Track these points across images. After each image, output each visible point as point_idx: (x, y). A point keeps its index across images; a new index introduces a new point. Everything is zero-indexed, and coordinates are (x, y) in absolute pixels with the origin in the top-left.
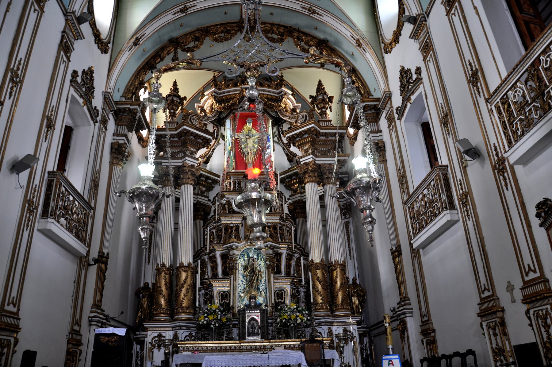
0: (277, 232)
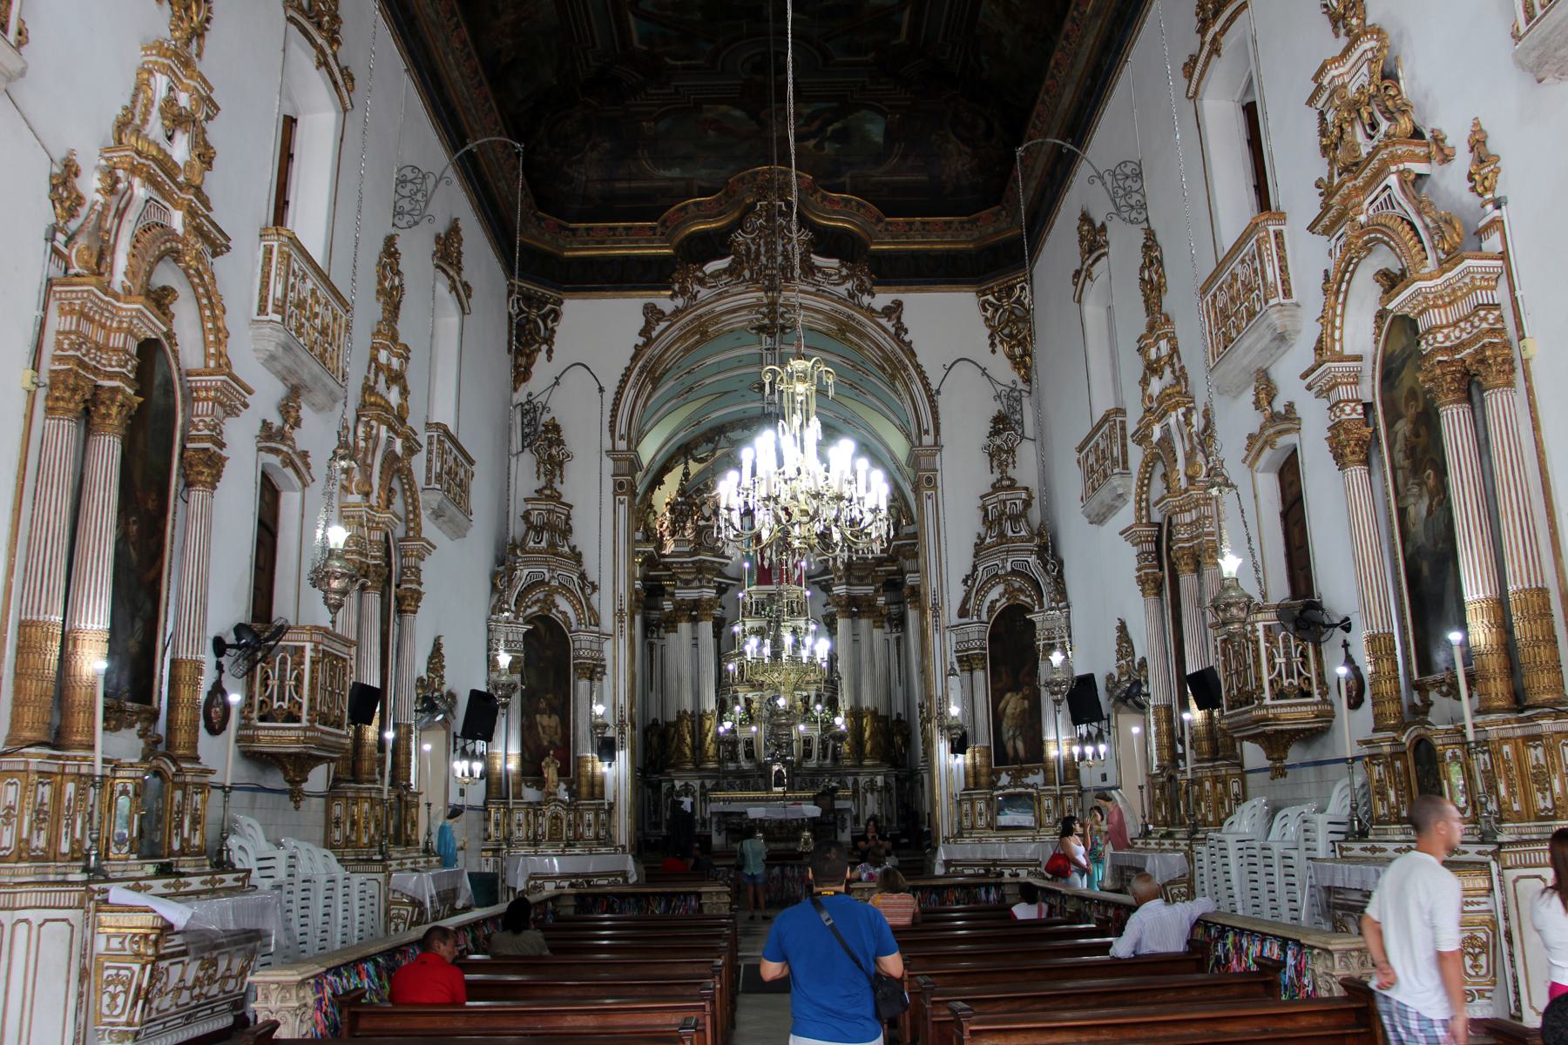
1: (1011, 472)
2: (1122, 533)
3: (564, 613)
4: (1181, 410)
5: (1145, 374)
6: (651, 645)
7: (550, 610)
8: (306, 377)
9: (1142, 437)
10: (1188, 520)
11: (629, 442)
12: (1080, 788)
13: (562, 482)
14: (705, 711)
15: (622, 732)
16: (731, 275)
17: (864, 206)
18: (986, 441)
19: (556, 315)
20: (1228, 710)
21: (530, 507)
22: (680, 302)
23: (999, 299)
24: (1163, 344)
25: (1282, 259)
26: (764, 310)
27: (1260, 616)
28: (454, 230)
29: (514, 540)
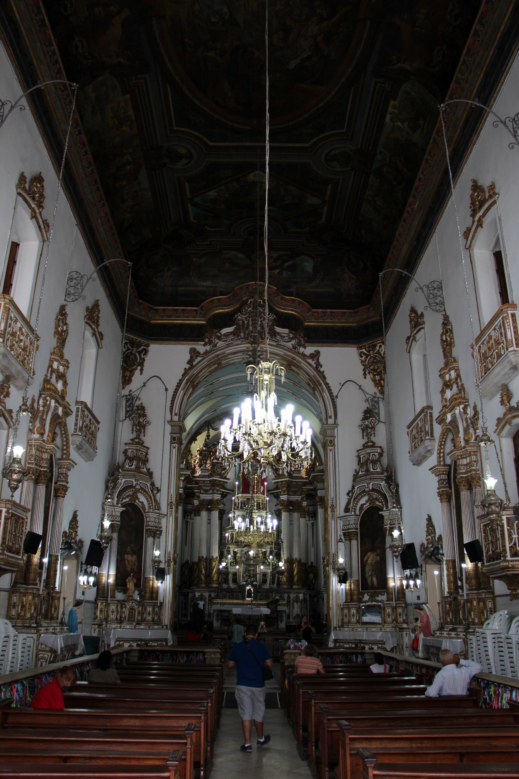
1: (373, 439)
2: (430, 470)
3: (142, 503)
4: (462, 406)
5: (443, 388)
6: (187, 523)
7: (135, 501)
8: (13, 371)
9: (441, 420)
10: (465, 463)
11: (180, 417)
12: (406, 603)
13: (144, 436)
14: (213, 557)
15: (169, 566)
16: (234, 335)
17: (302, 303)
18: (360, 423)
19: (146, 352)
20: (487, 562)
21: (127, 447)
22: (208, 348)
23: (368, 351)
24: (453, 372)
25: (515, 327)
26: (250, 353)
27: (504, 512)
28: (96, 305)
29: (118, 463)
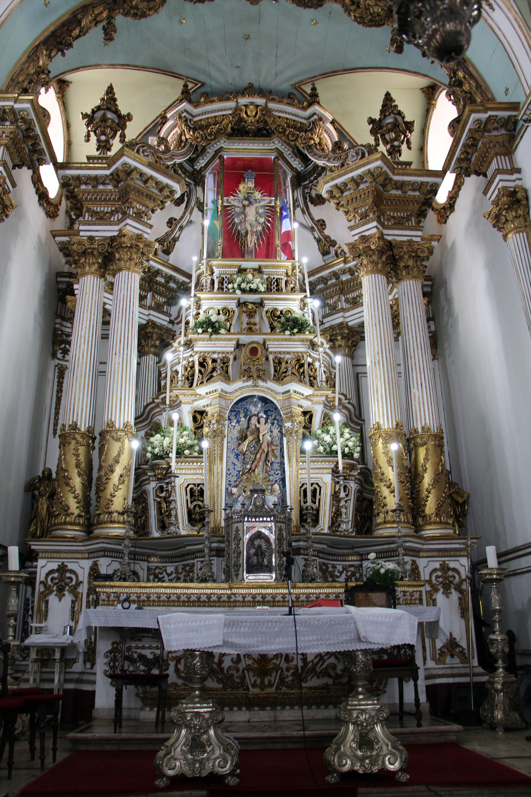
0: (303, 372)
14: (111, 425)
